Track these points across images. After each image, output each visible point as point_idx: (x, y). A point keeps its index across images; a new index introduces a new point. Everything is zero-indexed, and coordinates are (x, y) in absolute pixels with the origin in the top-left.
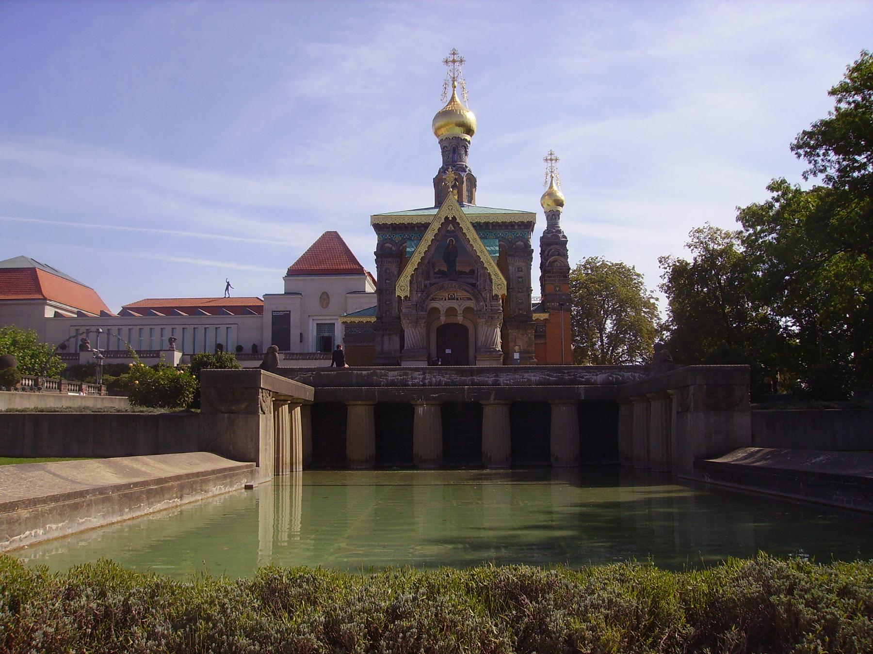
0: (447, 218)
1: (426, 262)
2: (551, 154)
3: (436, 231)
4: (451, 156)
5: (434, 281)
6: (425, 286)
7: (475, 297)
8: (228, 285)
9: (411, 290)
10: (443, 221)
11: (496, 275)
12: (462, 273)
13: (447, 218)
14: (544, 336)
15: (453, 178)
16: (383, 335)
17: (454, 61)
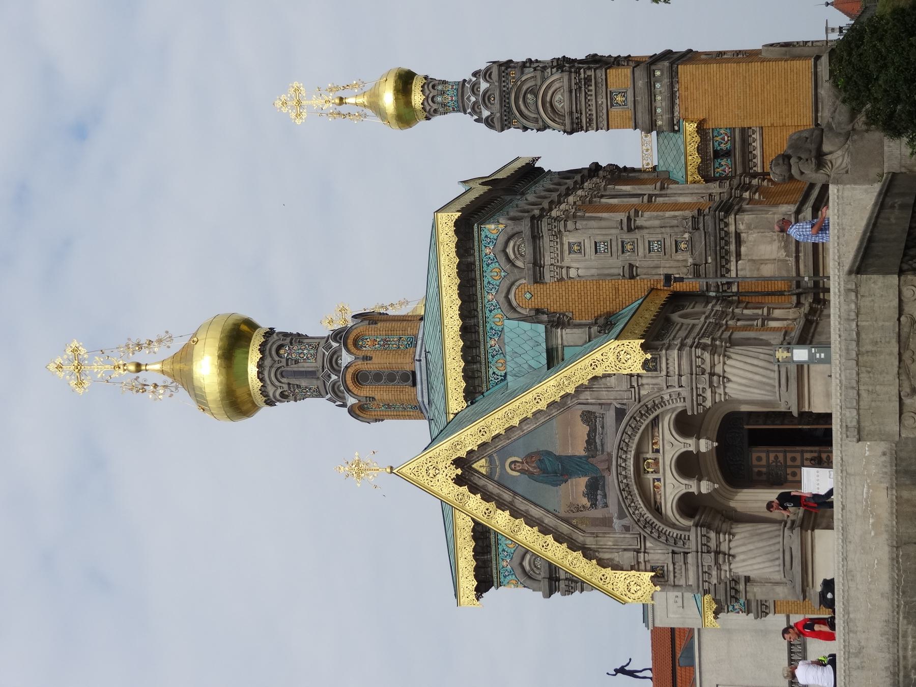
1: (565, 528)
3: (492, 506)
4: (304, 383)
5: (613, 509)
6: (627, 529)
7: (649, 411)
8: (622, 670)
10: (465, 489)
11: (594, 366)
12: (590, 441)
13: (459, 481)
14: (743, 131)
15: (361, 367)
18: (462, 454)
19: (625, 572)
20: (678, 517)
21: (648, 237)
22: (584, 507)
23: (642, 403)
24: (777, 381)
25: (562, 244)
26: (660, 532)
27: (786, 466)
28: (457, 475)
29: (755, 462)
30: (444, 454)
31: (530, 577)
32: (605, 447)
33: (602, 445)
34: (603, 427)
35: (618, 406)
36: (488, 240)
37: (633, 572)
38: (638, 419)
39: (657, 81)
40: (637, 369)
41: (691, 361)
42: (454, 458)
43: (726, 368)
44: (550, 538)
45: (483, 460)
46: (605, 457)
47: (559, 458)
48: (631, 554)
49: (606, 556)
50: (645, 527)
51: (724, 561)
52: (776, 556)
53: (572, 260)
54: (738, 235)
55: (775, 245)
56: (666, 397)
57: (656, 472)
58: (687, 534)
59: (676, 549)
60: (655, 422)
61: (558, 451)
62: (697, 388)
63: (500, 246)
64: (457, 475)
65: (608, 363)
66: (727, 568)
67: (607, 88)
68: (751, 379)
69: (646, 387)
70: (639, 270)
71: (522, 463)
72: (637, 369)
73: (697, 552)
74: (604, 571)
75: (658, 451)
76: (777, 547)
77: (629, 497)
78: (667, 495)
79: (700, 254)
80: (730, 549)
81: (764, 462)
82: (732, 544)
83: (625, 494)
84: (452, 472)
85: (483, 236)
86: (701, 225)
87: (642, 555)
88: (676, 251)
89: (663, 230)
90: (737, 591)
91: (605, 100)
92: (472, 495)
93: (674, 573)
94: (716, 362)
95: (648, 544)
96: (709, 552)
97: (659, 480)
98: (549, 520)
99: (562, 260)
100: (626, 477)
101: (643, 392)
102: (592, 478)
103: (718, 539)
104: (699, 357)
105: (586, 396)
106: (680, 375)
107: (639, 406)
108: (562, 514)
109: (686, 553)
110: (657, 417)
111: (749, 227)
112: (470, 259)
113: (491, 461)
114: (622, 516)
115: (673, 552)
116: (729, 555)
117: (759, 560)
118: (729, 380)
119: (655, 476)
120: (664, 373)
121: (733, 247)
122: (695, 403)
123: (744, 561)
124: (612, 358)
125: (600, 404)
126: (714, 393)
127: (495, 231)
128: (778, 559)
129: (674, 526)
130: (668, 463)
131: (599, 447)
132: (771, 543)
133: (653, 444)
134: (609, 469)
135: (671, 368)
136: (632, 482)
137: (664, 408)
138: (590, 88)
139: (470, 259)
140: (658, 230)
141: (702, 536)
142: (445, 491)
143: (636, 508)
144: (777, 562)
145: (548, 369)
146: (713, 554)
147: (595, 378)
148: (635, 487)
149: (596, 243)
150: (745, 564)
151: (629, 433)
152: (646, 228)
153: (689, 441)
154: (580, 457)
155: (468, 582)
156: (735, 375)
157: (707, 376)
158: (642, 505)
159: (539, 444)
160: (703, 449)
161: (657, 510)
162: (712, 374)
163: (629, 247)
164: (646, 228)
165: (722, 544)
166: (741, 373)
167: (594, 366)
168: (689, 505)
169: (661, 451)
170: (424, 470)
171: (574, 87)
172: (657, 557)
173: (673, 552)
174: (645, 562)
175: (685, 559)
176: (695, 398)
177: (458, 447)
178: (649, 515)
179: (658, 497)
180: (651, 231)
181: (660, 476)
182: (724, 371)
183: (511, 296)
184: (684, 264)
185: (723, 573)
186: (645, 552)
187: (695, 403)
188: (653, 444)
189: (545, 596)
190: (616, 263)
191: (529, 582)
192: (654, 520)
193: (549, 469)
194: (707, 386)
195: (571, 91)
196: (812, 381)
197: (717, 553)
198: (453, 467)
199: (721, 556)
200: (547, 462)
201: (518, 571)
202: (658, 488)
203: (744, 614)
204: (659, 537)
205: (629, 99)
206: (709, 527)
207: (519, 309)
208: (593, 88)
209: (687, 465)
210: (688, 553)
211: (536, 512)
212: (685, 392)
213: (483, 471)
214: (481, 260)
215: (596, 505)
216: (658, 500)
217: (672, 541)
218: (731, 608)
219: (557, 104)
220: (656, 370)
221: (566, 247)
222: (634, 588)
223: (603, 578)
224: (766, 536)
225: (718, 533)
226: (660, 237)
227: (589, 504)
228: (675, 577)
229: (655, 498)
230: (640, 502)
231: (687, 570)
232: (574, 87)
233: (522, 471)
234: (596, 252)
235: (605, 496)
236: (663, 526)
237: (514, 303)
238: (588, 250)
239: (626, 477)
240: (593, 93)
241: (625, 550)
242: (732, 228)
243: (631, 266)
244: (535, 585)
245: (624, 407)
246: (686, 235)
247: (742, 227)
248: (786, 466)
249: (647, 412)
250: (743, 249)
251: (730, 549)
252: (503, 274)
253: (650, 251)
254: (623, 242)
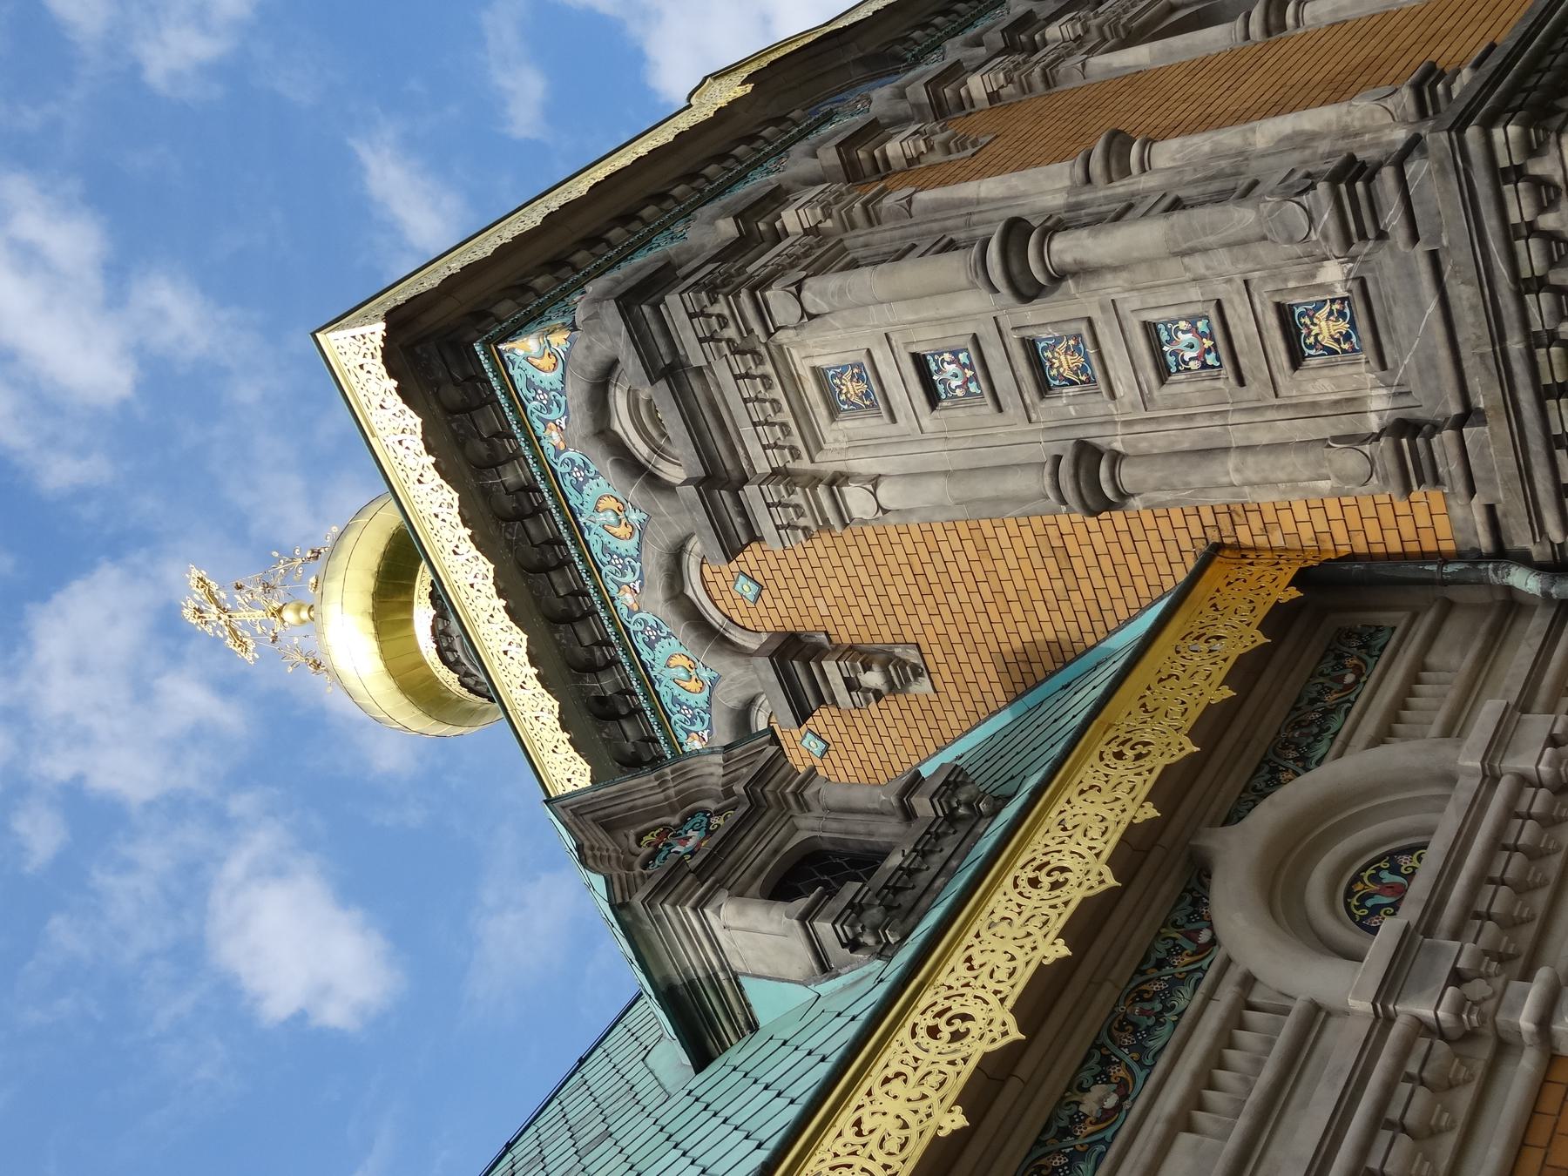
25: (792, 381)
53: (855, 445)
70: (1127, 475)
79: (1427, 366)
86: (1393, 217)
88: (1296, 359)
89: (1198, 264)
99: (815, 444)
140: (1173, 268)
145: (701, 1059)
149: (920, 362)
152: (1115, 269)
163: (1062, 362)
180: (1142, 275)
183: (694, 590)
184: (1344, 426)
190: (1027, 435)
207: (736, 636)
214: (550, 474)
221: (811, 389)
234: (933, 398)
237: (716, 618)
238: (897, 396)
243: (1087, 454)
252: (634, 517)
253: (1163, 372)
254: (1030, 346)
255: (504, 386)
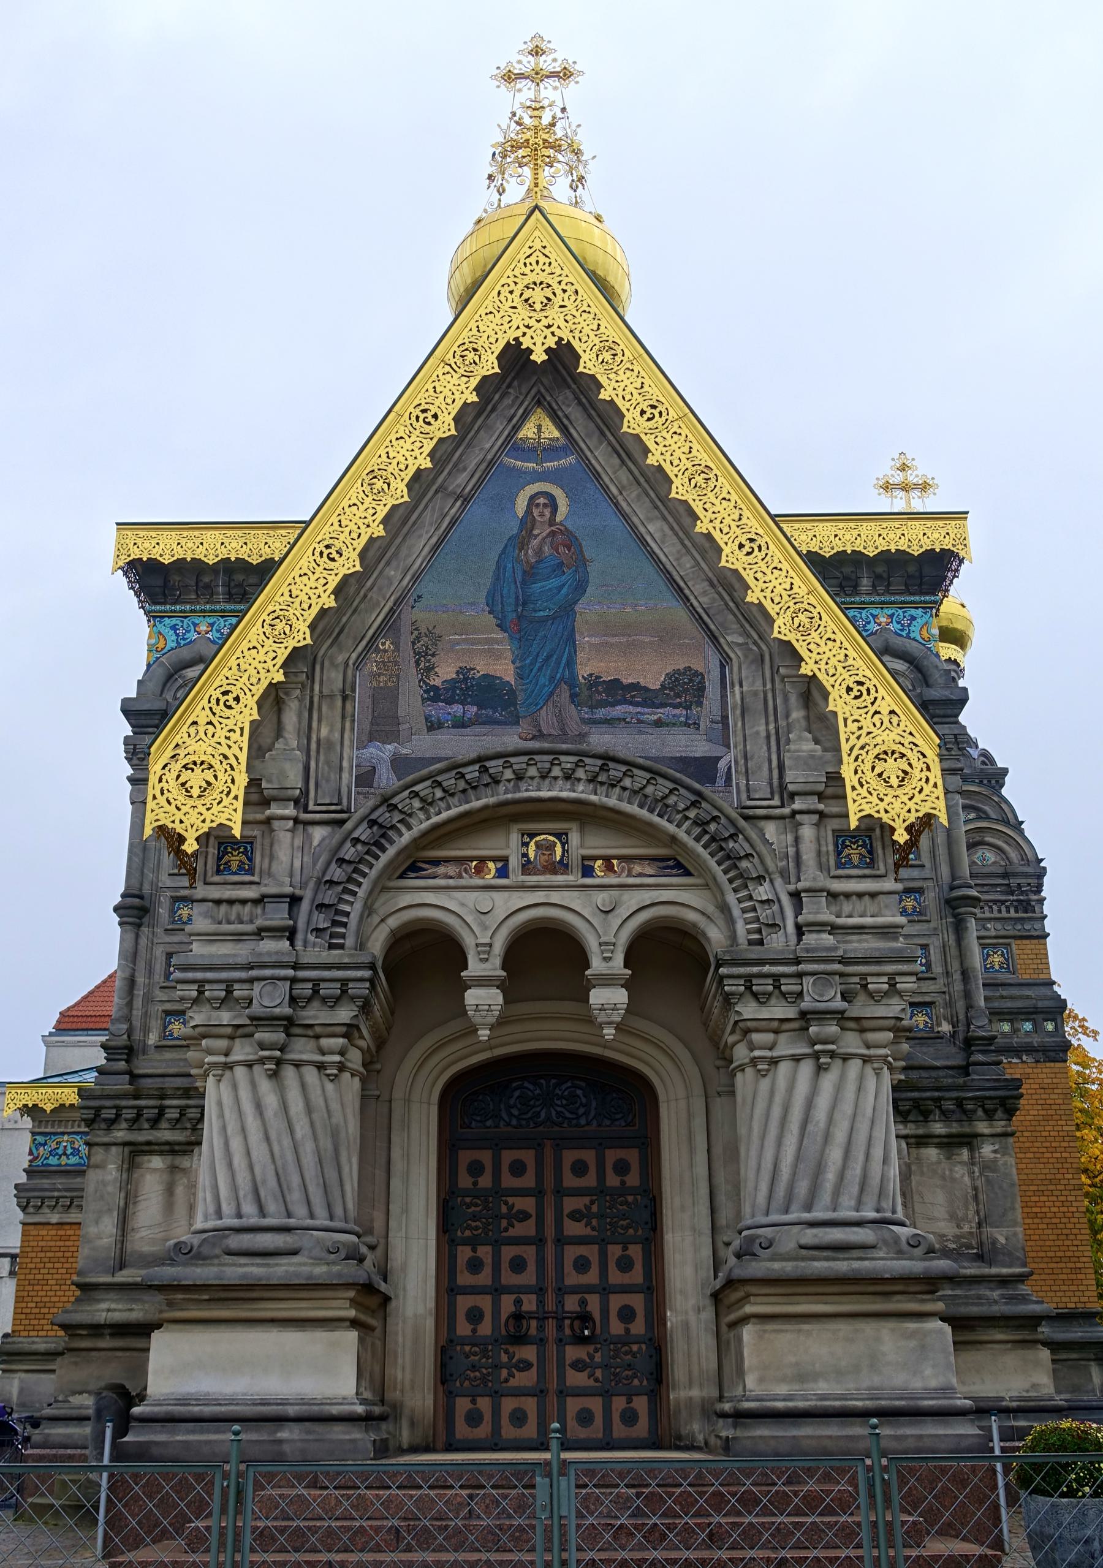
0: (514, 356)
2: (903, 468)
3: (445, 427)
5: (422, 744)
6: (365, 778)
7: (715, 842)
9: (257, 796)
10: (490, 365)
12: (617, 691)
13: (514, 356)
16: (135, 1152)
17: (537, 77)
18: (588, 364)
19: (243, 757)
20: (393, 922)
21: (935, 945)
22: (430, 669)
23: (742, 823)
24: (829, 1215)
26: (356, 867)
27: (497, 1244)
28: (530, 351)
29: (508, 1156)
30: (586, 325)
31: (170, 677)
32: (603, 728)
33: (608, 722)
34: (658, 723)
35: (722, 765)
36: (906, 622)
37: (242, 779)
38: (692, 814)
39: (1035, 1025)
40: (858, 807)
41: (878, 961)
42: (576, 344)
43: (855, 1065)
44: (349, 563)
45: (556, 434)
46: (574, 727)
47: (567, 611)
48: (294, 779)
49: (290, 719)
50: (373, 823)
51: (262, 1046)
52: (271, 1207)
54: (969, 1140)
55: (948, 1229)
56: (763, 892)
57: (527, 867)
58: (349, 942)
59: (305, 906)
60: (675, 864)
61: (587, 611)
62: (800, 975)
63: (897, 642)
64: (530, 351)
65: (867, 723)
66: (233, 1058)
67: (1015, 937)
68: (827, 1137)
69: (790, 838)
71: (552, 522)
72: (858, 807)
73: (296, 967)
74: (250, 702)
75: (588, 872)
76: (300, 1210)
77: (462, 785)
78: (458, 895)
80: (298, 1065)
81: (508, 1181)
82: (311, 1075)
83: (472, 772)
84: (539, 340)
85: (913, 612)
87: (290, 811)
89: (957, 976)
90: (112, 1123)
91: (993, 933)
92: (474, 382)
93: (231, 902)
94: (871, 1036)
95: (318, 834)
96: (293, 1000)
97: (503, 873)
98: (395, 576)
100: (519, 777)
101: (771, 830)
102: (512, 692)
103: (330, 1031)
104: (892, 985)
105: (749, 682)
106: (833, 929)
107: (734, 815)
108: (409, 616)
109: (291, 934)
110: (704, 869)
111: (988, 1166)
112: (865, 583)
113: (551, 451)
114: (399, 764)
115: (294, 900)
116: (279, 1062)
117: (259, 1152)
118: (820, 1069)
119: (514, 862)
120: (837, 886)
121: (938, 1128)
122: (755, 970)
123: (259, 1107)
124: (888, 738)
125: (725, 719)
126: (778, 1027)
127: (925, 634)
128: (262, 1213)
129: (368, 909)
130: (555, 897)
131: (601, 713)
132: (311, 1189)
133: (607, 859)
134: (540, 736)
135: (847, 907)
136: (503, 794)
137: (727, 888)
138: (1012, 910)
139: (865, 583)
141: (344, 982)
142: (489, 326)
143: (427, 803)
144: (249, 1208)
146: (287, 1011)
147: (812, 692)
148: (492, 800)
150: (248, 1107)
151: (650, 790)
152: (959, 940)
153: (619, 959)
154: (571, 663)
155: (167, 549)
156: (839, 1089)
157: (839, 1004)
158: (435, 819)
159: (600, 562)
160: (598, 996)
161: (412, 865)
162: (840, 1016)
164: (959, 940)
165: (312, 1043)
166: (847, 1107)
167: (858, 689)
168: (426, 958)
169: (588, 881)
170: (543, 277)
171: (1014, 882)
172: (283, 854)
173: (294, 900)
174: (268, 821)
175: (275, 932)
176: (766, 969)
177: (607, 356)
178: (407, 837)
179: (451, 870)
180: (954, 951)
181: (516, 876)
182: (846, 1058)
185: (223, 1043)
186: (296, 821)
187: (755, 970)
188: (607, 859)
189: (125, 701)
191: (160, 673)
192: (391, 851)
193: (536, 587)
194: (806, 1004)
195: (1005, 875)
196: (844, 1327)
197: (289, 1024)
198: (551, 342)
199: (280, 1037)
200: (554, 582)
201: (186, 654)
202: (479, 871)
203: (26, 1165)
204: (341, 861)
205: (999, 975)
206: (366, 1008)
208: (1012, 914)
209: (545, 955)
210: (291, 939)
211: (419, 546)
212: (778, 942)
213: (528, 431)
215: (435, 699)
216: (441, 870)
217: (329, 897)
218: (40, 1139)
219: (979, 854)
220: (839, 865)
222: (196, 779)
223: (229, 699)
224: (331, 1175)
225: (350, 1031)
226: (937, 969)
227: (437, 682)
228: (218, 902)
229: (448, 860)
230: (445, 815)
231: (239, 937)
232: (1014, 882)
233: (528, 523)
235: (461, 724)
236: (373, 873)
239: (519, 777)
240: (1004, 914)
241: (307, 769)
242: (982, 1127)
244: (153, 686)
245: (720, 781)
246: (946, 1028)
247: (987, 1150)
248: (497, 1244)
249: (713, 839)
250: (932, 1153)
251: (298, 1065)
254: (920, 891)
255: (914, 602)
